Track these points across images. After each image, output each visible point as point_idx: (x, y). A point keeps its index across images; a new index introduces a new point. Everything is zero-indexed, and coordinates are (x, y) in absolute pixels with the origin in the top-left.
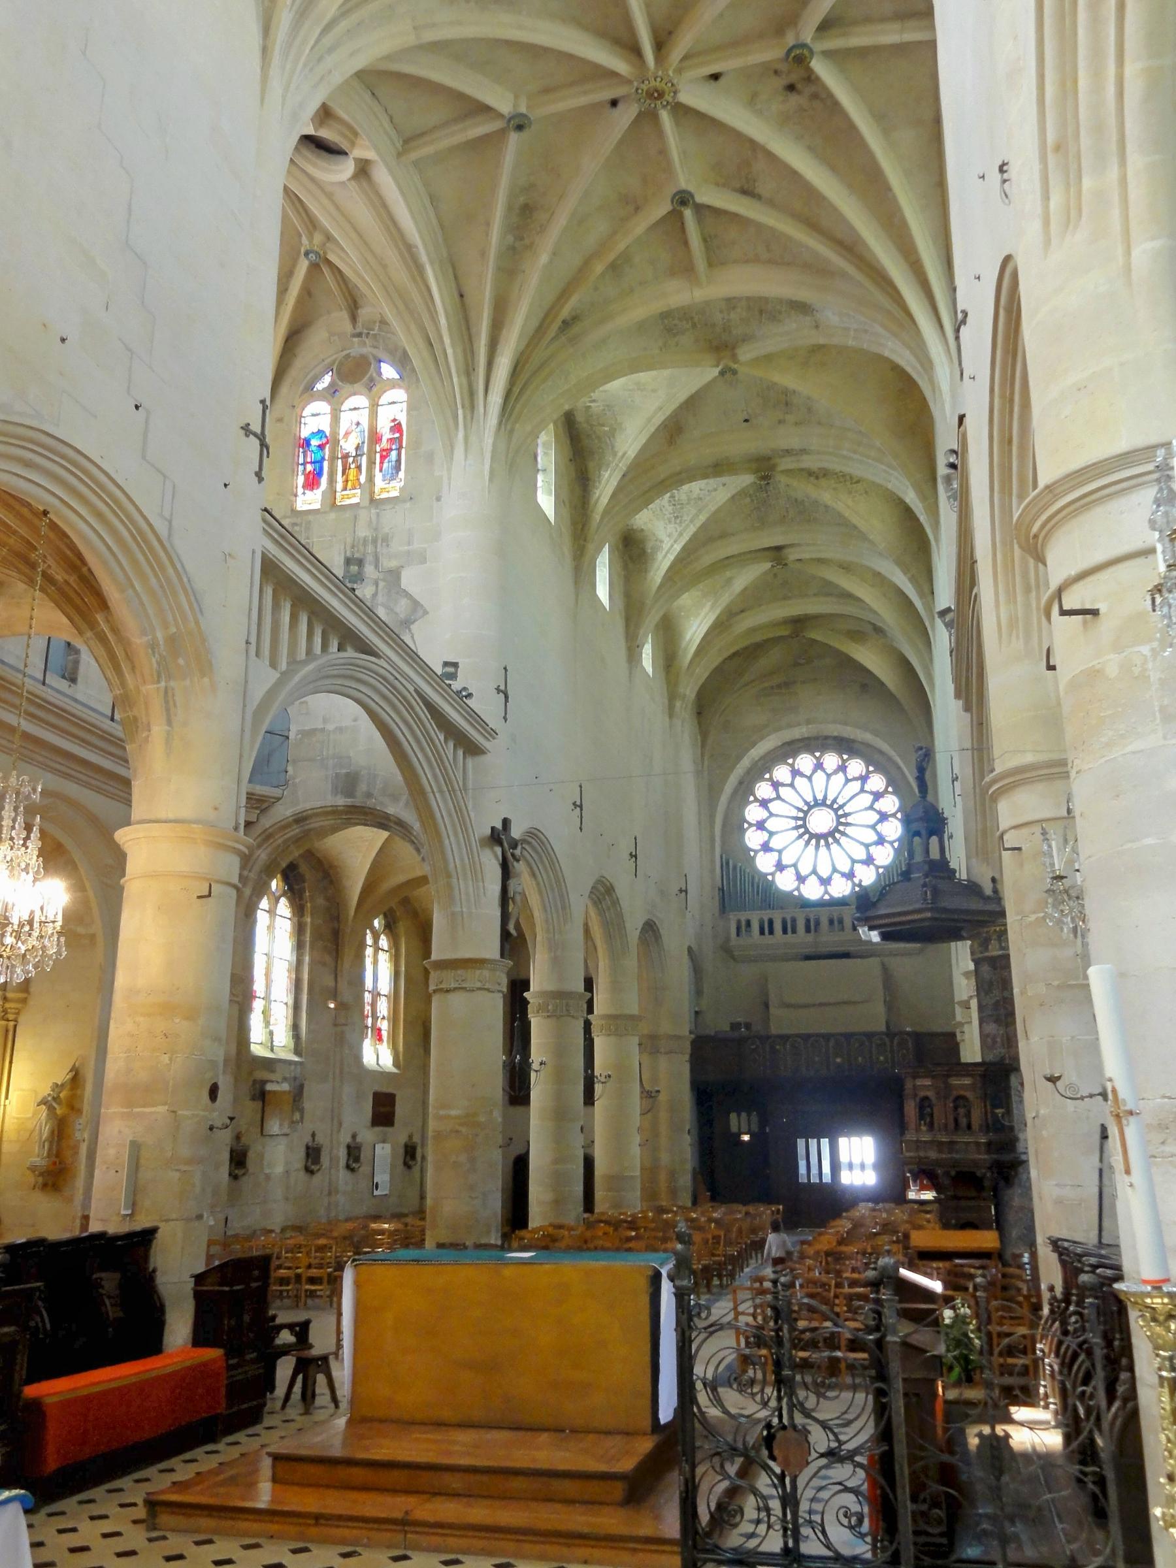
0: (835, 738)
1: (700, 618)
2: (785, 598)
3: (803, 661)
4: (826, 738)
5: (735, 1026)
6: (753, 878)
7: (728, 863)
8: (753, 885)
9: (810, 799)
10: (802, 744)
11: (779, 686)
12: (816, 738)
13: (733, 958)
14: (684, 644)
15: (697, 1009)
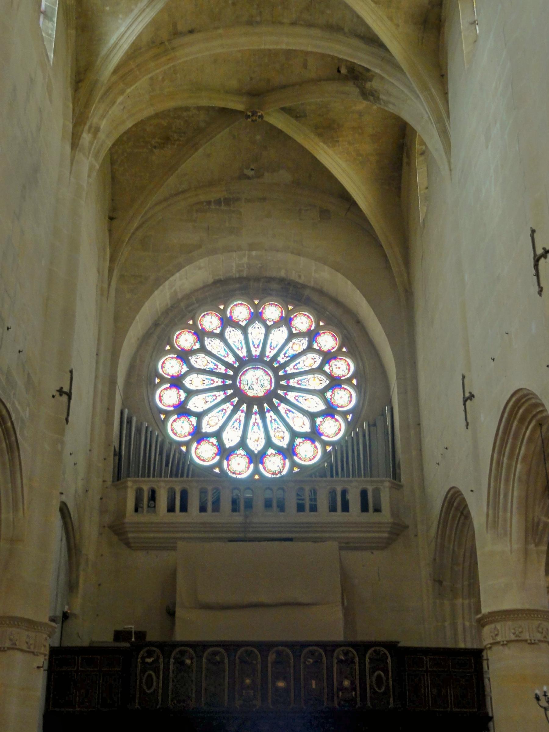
0: (282, 280)
1: (129, 20)
2: (250, 23)
3: (250, 173)
4: (270, 280)
5: (119, 635)
6: (163, 442)
7: (129, 422)
8: (161, 454)
9: (243, 353)
10: (237, 286)
11: (218, 202)
12: (257, 279)
13: (128, 544)
14: (104, 51)
15: (66, 609)
